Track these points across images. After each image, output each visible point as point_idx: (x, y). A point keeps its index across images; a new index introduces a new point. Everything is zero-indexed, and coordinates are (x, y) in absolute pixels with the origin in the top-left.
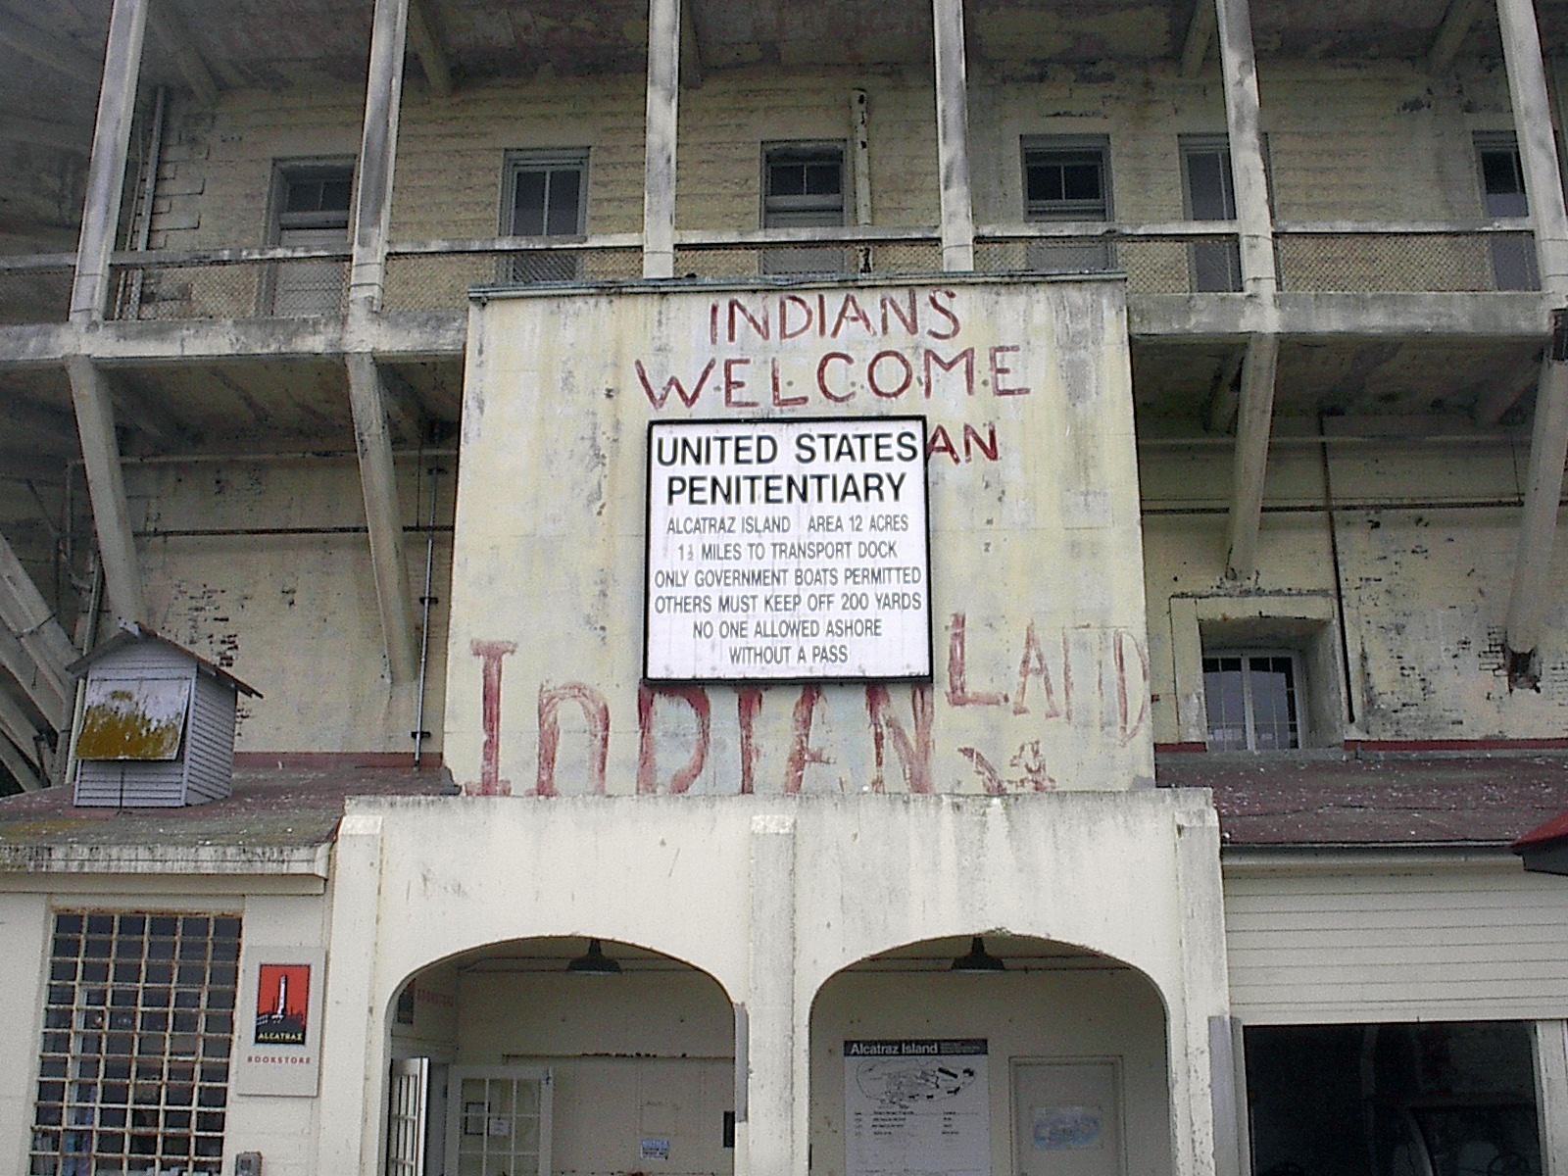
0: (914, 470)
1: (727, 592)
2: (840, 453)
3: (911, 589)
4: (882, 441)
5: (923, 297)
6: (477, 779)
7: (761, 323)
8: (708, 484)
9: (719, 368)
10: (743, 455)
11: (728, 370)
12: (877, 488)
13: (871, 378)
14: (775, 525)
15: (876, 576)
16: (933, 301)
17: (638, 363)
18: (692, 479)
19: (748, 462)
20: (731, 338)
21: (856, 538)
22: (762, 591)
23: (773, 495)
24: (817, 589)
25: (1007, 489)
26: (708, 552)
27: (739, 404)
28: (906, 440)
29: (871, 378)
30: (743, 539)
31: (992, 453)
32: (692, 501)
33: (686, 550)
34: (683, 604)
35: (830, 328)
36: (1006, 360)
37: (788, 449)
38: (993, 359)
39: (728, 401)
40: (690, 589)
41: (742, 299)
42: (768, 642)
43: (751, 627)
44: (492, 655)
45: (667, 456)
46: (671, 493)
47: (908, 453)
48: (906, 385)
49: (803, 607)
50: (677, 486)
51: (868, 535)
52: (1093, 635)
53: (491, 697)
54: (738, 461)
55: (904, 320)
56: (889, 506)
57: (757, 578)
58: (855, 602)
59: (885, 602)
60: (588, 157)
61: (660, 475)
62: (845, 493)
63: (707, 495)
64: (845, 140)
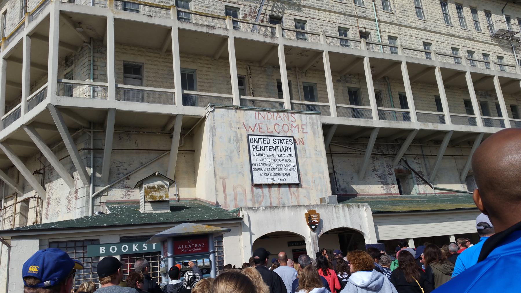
0: (293, 146)
1: (265, 167)
2: (280, 143)
3: (294, 168)
4: (287, 141)
5: (290, 114)
6: (223, 204)
7: (263, 116)
8: (259, 147)
9: (257, 125)
10: (265, 142)
11: (259, 125)
12: (287, 149)
13: (283, 129)
14: (272, 155)
15: (289, 165)
16: (291, 115)
17: (243, 123)
18: (257, 146)
19: (266, 143)
20: (259, 119)
21: (285, 158)
22: (271, 168)
23: (270, 150)
24: (280, 167)
25: (306, 150)
26: (261, 160)
27: (262, 132)
28: (291, 141)
29: (283, 129)
30: (267, 158)
31: (303, 144)
32: (257, 150)
33: (257, 159)
34: (258, 170)
35: (275, 119)
36: (304, 127)
37: (272, 141)
38: (302, 126)
39: (260, 131)
40: (259, 167)
41: (260, 112)
42: (273, 177)
43: (270, 174)
44: (224, 179)
45: (252, 142)
46: (253, 148)
47: (291, 143)
48: (288, 131)
49: (277, 171)
50: (254, 147)
51: (287, 158)
52: (322, 176)
53: (224, 187)
54: (264, 143)
55: (287, 118)
56: (289, 153)
57: (270, 165)
58: (286, 170)
59: (291, 170)
60: (195, 72)
61: (251, 145)
62: (282, 150)
63: (259, 149)
64: (245, 76)
